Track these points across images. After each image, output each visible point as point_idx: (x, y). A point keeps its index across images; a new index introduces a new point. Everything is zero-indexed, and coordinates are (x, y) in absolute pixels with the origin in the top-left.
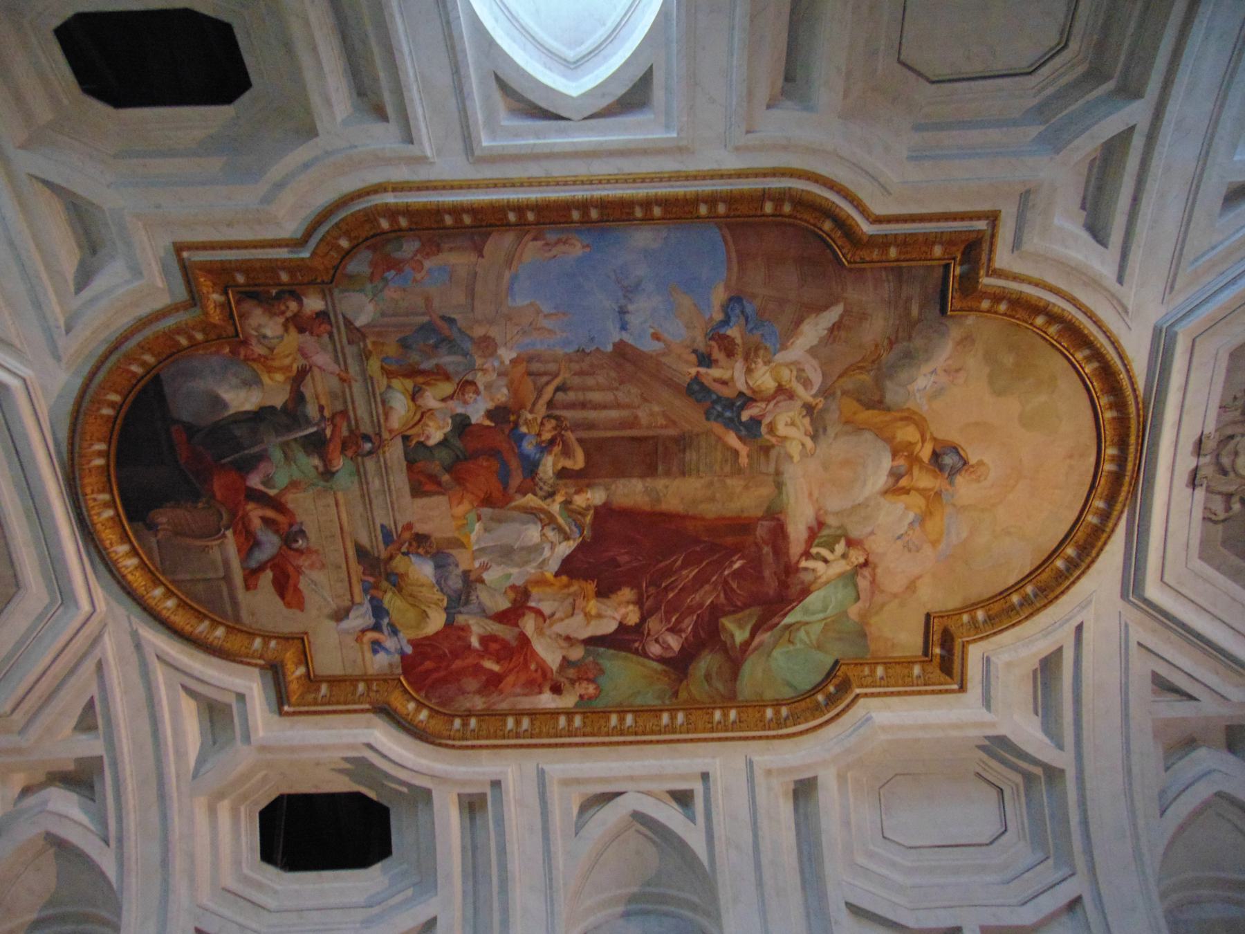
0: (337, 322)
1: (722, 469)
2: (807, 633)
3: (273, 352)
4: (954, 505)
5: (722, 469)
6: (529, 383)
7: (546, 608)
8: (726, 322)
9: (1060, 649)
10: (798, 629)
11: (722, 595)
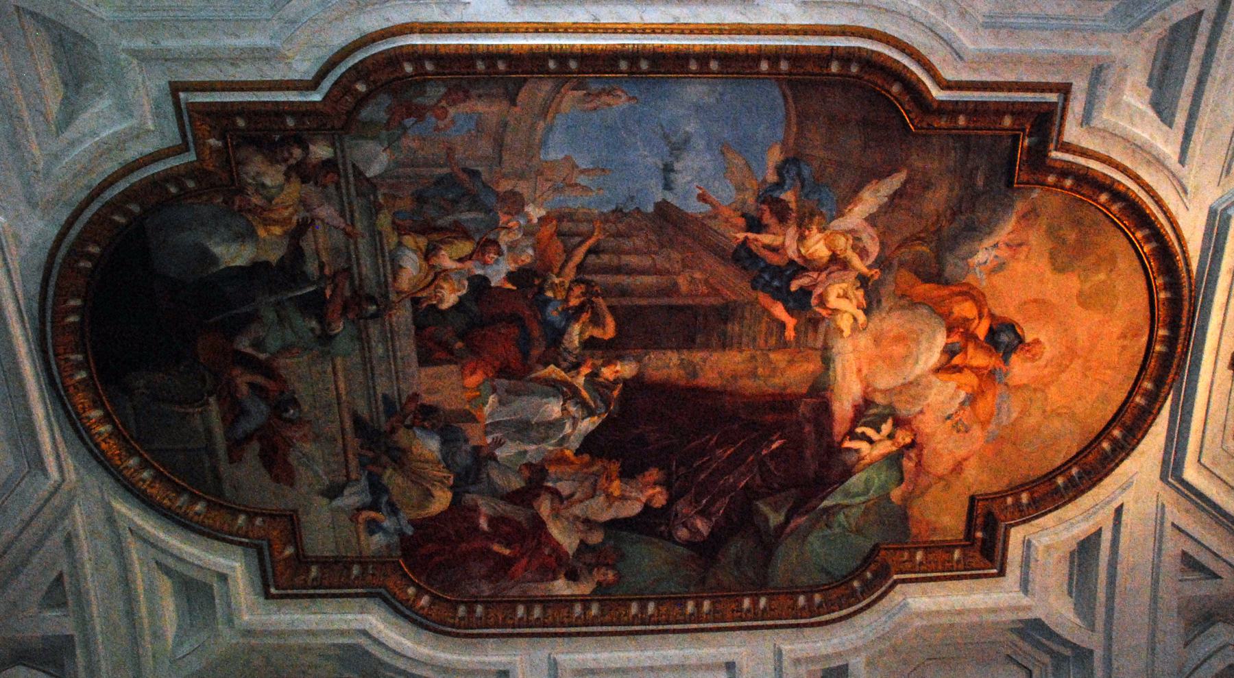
0: (345, 170)
1: (766, 342)
2: (846, 516)
3: (270, 202)
4: (1006, 384)
5: (766, 342)
6: (558, 244)
7: (565, 488)
8: (779, 185)
9: (1098, 533)
10: (838, 513)
11: (758, 477)
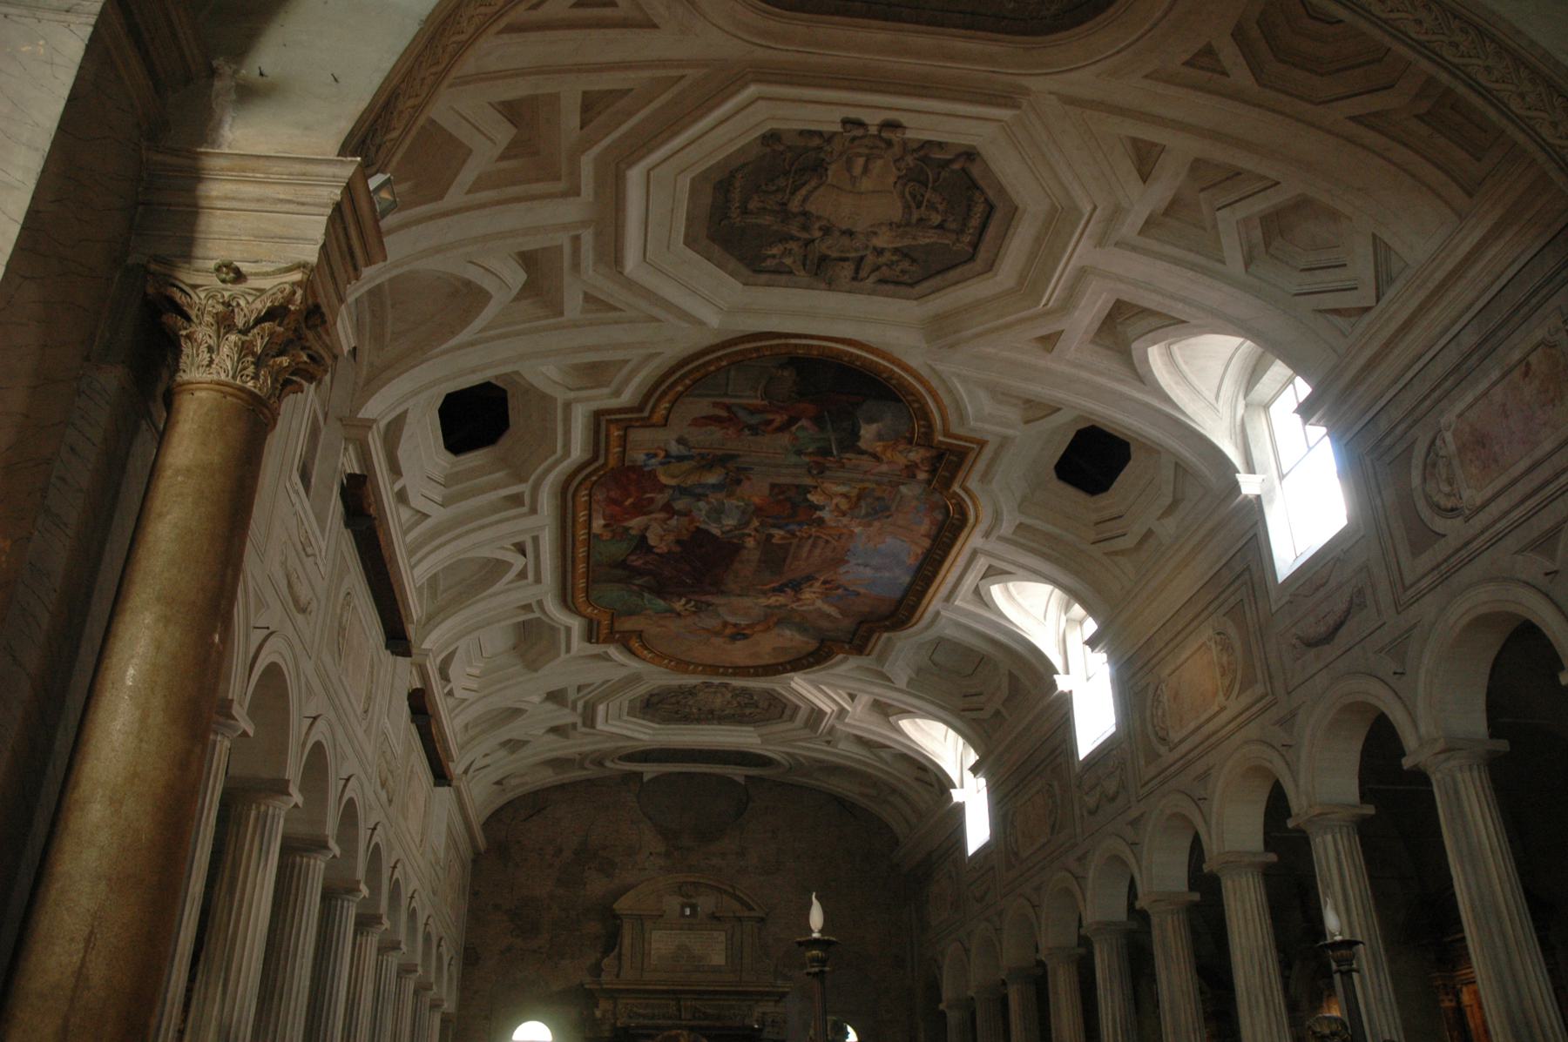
7: (673, 522)
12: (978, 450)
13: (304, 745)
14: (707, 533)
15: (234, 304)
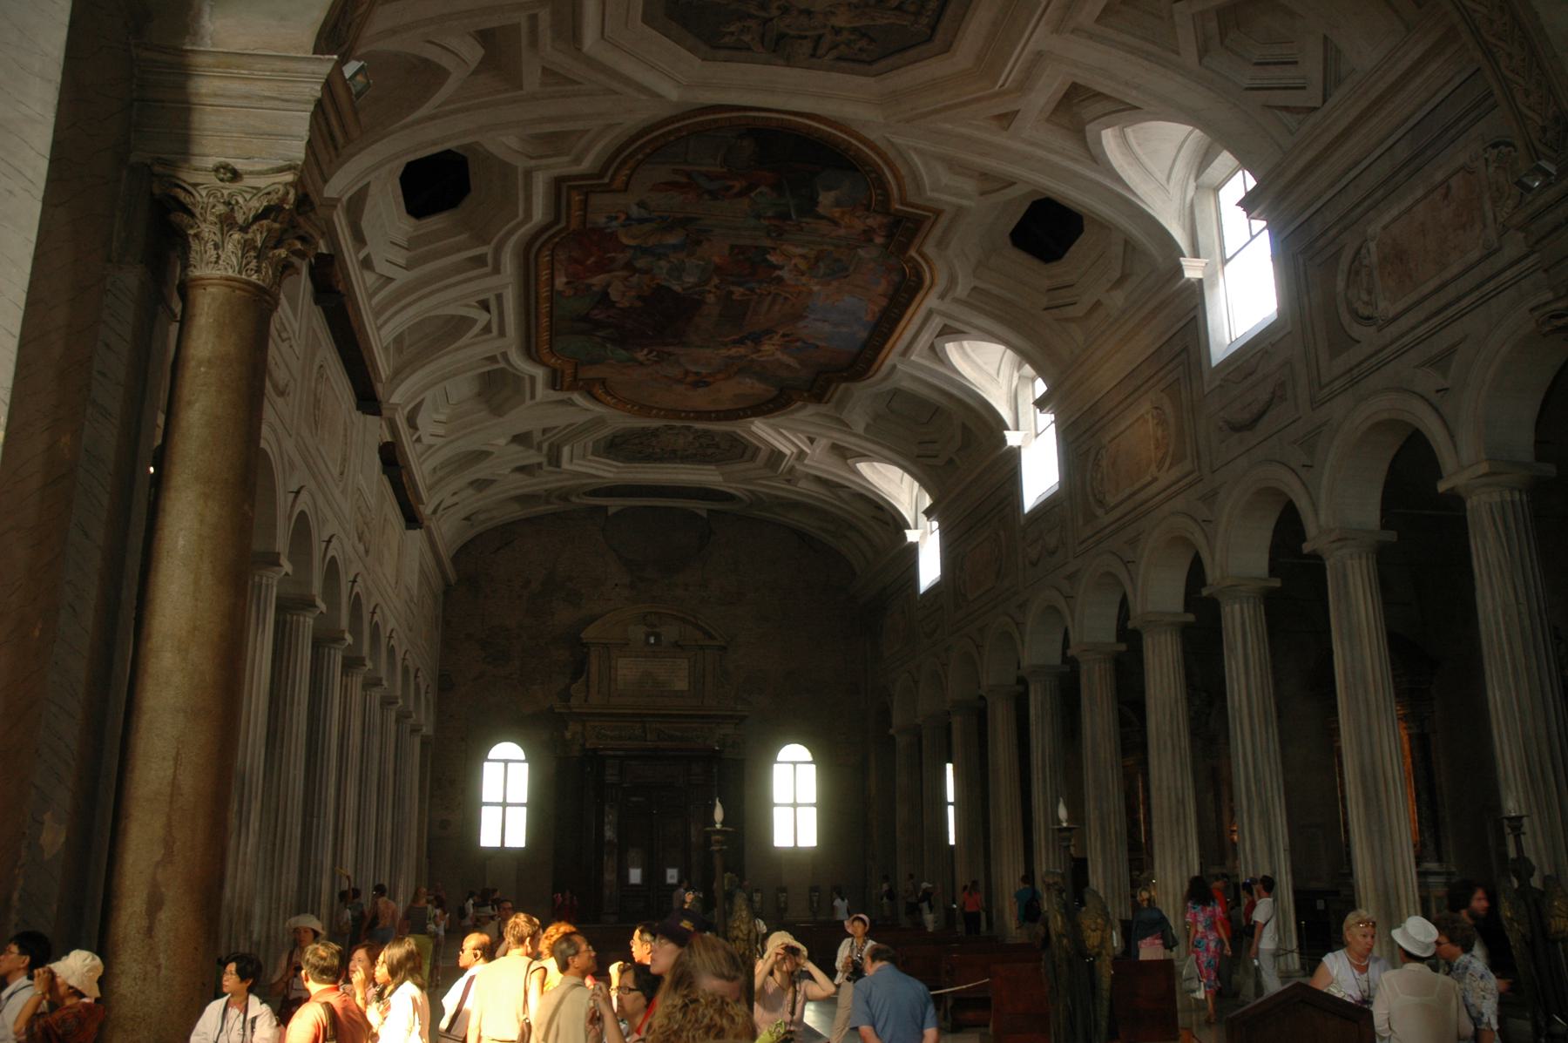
7: (635, 279)
12: (932, 220)
13: (290, 517)
14: (669, 289)
15: (233, 202)
